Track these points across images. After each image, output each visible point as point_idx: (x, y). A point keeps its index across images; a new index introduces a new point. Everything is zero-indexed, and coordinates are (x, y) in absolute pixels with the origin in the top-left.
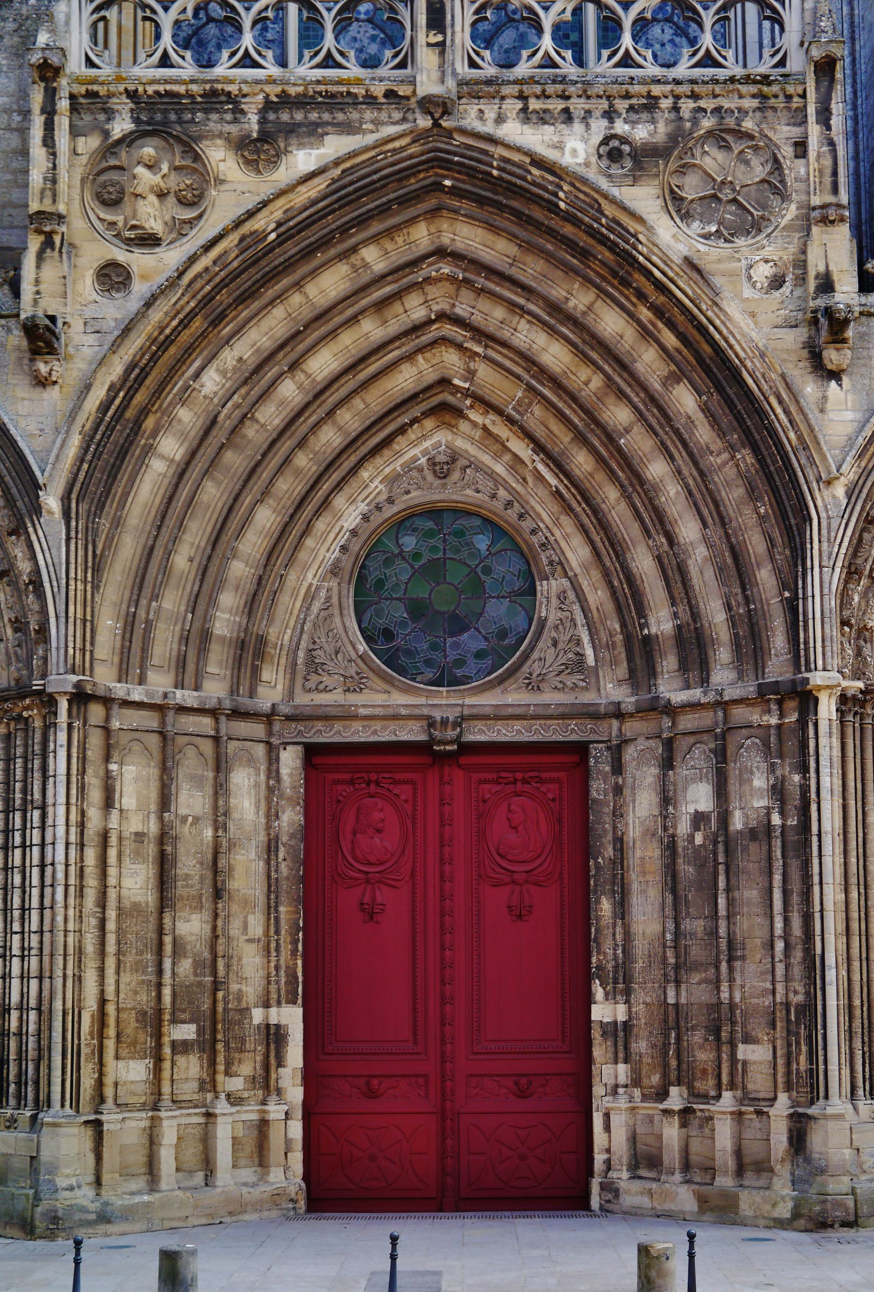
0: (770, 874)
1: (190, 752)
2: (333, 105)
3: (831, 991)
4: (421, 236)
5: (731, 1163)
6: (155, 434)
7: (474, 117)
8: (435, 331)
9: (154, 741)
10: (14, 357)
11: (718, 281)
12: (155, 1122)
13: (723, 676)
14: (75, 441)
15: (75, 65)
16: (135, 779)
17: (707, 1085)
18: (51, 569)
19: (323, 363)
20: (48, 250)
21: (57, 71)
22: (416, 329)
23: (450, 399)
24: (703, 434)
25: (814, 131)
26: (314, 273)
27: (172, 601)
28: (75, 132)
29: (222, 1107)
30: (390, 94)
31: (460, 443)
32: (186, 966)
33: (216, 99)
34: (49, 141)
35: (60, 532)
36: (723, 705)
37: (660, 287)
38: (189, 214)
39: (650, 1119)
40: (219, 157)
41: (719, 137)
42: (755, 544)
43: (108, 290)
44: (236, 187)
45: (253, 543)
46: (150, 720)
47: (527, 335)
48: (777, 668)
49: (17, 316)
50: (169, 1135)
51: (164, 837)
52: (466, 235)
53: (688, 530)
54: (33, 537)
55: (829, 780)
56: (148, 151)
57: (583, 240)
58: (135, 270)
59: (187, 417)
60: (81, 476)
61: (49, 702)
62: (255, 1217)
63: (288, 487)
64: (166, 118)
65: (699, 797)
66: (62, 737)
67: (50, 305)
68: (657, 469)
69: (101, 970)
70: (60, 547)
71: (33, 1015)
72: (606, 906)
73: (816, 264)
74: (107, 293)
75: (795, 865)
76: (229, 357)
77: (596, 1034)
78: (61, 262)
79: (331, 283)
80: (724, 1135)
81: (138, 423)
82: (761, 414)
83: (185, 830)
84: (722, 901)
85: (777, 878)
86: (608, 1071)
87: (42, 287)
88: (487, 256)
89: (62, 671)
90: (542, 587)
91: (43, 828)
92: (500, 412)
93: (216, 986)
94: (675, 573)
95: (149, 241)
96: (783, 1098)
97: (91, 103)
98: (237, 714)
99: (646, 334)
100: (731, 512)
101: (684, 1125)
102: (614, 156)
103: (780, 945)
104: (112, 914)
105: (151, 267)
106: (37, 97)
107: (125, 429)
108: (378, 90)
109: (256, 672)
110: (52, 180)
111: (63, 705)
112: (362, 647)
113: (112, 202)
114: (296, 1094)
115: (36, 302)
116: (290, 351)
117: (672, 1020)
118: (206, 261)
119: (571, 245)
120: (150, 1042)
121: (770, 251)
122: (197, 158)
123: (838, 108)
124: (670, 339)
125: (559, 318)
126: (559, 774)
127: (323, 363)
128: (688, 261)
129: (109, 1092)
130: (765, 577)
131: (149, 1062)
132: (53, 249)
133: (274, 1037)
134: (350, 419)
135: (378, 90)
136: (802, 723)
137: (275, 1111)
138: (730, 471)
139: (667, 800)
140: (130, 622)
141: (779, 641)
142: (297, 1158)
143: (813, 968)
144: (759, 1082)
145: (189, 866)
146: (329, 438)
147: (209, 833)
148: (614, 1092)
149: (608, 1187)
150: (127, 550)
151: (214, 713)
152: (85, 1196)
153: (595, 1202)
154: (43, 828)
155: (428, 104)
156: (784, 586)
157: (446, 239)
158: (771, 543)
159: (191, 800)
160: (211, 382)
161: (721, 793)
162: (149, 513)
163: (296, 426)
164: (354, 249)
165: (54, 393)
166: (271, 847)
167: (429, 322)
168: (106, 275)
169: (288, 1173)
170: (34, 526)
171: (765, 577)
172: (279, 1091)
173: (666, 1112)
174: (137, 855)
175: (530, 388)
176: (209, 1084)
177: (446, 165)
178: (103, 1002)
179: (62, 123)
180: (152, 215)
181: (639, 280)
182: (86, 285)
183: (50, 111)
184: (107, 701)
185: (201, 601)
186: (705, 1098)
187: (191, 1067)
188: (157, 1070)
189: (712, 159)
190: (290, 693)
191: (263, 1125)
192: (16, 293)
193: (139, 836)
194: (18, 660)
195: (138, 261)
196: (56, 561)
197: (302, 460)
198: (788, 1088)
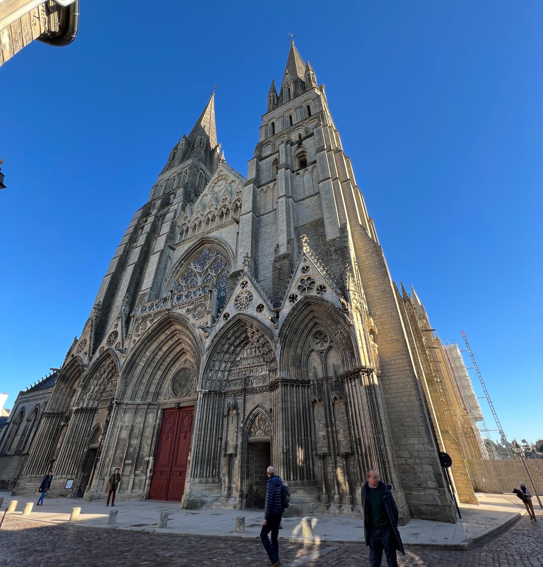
1: (141, 412)
14: (125, 365)
19: (165, 348)
27: (142, 387)
28: (135, 323)
45: (158, 377)
59: (144, 359)
62: (133, 500)
63: (163, 368)
64: (144, 319)
67: (127, 347)
79: (163, 337)
81: (134, 362)
95: (139, 336)
105: (137, 339)
127: (165, 348)
134: (172, 356)
145: (136, 431)
146: (169, 359)
160: (148, 354)
163: (163, 359)
164: (164, 331)
167: (177, 340)
169: (144, 491)
172: (146, 474)
174: (125, 430)
176: (131, 472)
193: (127, 426)
197: (165, 363)
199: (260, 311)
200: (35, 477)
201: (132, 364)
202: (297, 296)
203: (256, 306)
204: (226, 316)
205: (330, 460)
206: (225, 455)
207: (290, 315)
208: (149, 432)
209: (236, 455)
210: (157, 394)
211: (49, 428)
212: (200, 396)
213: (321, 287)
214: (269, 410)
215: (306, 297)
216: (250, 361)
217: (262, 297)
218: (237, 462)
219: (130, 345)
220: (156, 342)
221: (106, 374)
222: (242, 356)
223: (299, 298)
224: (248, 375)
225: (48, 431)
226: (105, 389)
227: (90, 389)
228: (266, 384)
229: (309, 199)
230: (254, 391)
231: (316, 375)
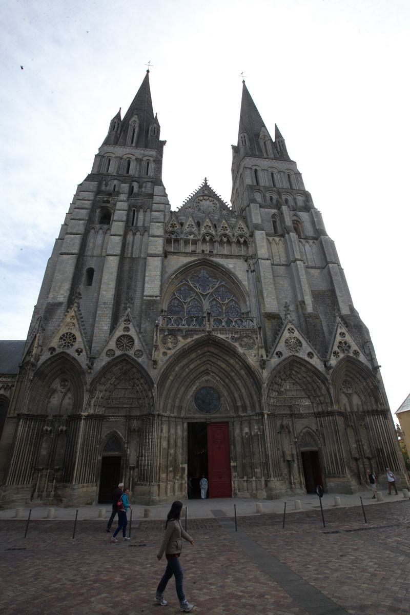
0: (258, 442)
2: (195, 331)
3: (270, 460)
4: (206, 349)
5: (255, 489)
6: (169, 376)
7: (214, 334)
8: (207, 362)
9: (167, 422)
11: (247, 356)
12: (167, 484)
13: (249, 412)
14: (159, 377)
15: (160, 325)
16: (165, 427)
17: (251, 476)
19: (192, 366)
21: (158, 326)
22: (205, 362)
23: (208, 371)
24: (245, 377)
25: (259, 336)
26: (191, 354)
28: (160, 334)
29: (176, 481)
30: (203, 330)
31: (209, 378)
32: (171, 458)
33: (180, 330)
34: (156, 335)
36: (250, 416)
37: (239, 356)
38: (175, 345)
39: (241, 482)
40: (180, 338)
41: (246, 337)
42: (253, 392)
44: (182, 342)
45: (181, 392)
46: (167, 419)
47: (220, 363)
48: (258, 411)
50: (169, 487)
51: (169, 437)
52: (212, 349)
53: (243, 391)
55: (267, 427)
56: (170, 337)
57: (228, 349)
61: (154, 416)
63: (186, 384)
64: (173, 333)
65: (246, 430)
66: (156, 421)
68: (238, 382)
69: (160, 459)
71: (149, 467)
72: (232, 447)
73: (260, 354)
75: (262, 440)
76: (179, 365)
77: (232, 468)
79: (193, 355)
80: (254, 484)
82: (254, 374)
83: (171, 436)
84: (251, 446)
85: (260, 442)
86: (234, 474)
88: (215, 352)
90: (221, 399)
91: (152, 436)
92: (215, 374)
93: (175, 461)
94: (241, 397)
95: (170, 349)
96: (263, 478)
97: (162, 330)
98: (179, 418)
99: (237, 363)
100: (249, 387)
101: (247, 483)
102: (233, 339)
103: (261, 453)
104: (162, 450)
105: (170, 353)
106: (155, 329)
108: (201, 329)
109: (181, 412)
110: (157, 340)
111: (156, 417)
112: (196, 407)
113: (165, 344)
114: (186, 479)
116: (187, 365)
117: (244, 466)
118: (178, 352)
119: (227, 351)
120: (166, 471)
121: (254, 352)
122: (177, 338)
123: (261, 333)
124: (241, 364)
125: (224, 361)
126: (224, 426)
127: (192, 366)
128: (243, 353)
129: (161, 479)
130: (255, 397)
131: (166, 474)
133: (183, 469)
134: (195, 374)
135: (201, 329)
136: (262, 418)
137: (184, 482)
138: (249, 382)
139: (241, 430)
140: (165, 403)
141: (257, 406)
142: (186, 490)
143: (267, 456)
144: (259, 475)
145: (172, 442)
146: (192, 377)
147: (174, 437)
148: (235, 478)
149: (236, 494)
150: (165, 393)
151: (175, 418)
152: (157, 498)
153: (233, 496)
154: (152, 436)
155: (208, 332)
156: (258, 398)
157: (209, 349)
158: (256, 392)
159: (172, 431)
160: (177, 369)
161: (250, 429)
165: (156, 370)
166: (183, 439)
169: (185, 493)
171: (255, 397)
173: (244, 481)
175: (220, 370)
176: (174, 478)
177: (210, 340)
178: (160, 464)
179: (158, 333)
180: (170, 345)
181: (236, 355)
182: (161, 355)
183: (157, 331)
184: (162, 416)
185: (174, 401)
186: (250, 478)
187: (171, 475)
188: (167, 475)
189: (245, 340)
190: (185, 415)
191: (182, 484)
192: (151, 356)
193: (165, 437)
195: (169, 352)
197: (188, 380)
198: (264, 476)
199: (311, 358)
200: (23, 488)
201: (164, 377)
202: (338, 353)
203: (307, 352)
204: (279, 354)
205: (360, 462)
206: (284, 461)
207: (337, 366)
208: (179, 441)
209: (294, 461)
210: (180, 408)
211: (28, 431)
212: (266, 416)
213: (355, 351)
214: (315, 430)
215: (348, 356)
216: (293, 393)
217: (310, 346)
218: (295, 465)
219: (162, 357)
220: (186, 359)
221: (112, 381)
222: (285, 388)
223: (342, 356)
224: (293, 403)
225: (28, 435)
226: (110, 396)
227: (95, 394)
228: (311, 412)
229: (313, 270)
230: (301, 416)
231: (345, 409)
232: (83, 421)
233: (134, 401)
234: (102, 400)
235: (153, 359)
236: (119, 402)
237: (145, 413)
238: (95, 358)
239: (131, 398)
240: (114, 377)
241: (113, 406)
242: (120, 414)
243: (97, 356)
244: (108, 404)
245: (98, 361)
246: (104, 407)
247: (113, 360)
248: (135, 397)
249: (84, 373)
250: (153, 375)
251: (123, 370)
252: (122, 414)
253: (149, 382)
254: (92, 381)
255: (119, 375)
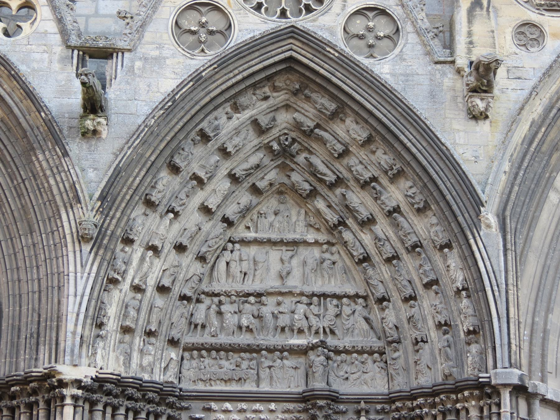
10: (449, 96)
18: (492, 275)
20: (478, 9)
35: (498, 244)
43: (524, 45)
49: (453, 62)
54: (475, 248)
58: (547, 29)
60: (513, 197)
70: (498, 256)
74: (523, 48)
78: (489, 19)
87: (475, 38)
89: (507, 365)
107: (542, 161)
111: (506, 397)
115: (469, 51)
132: (482, 8)
162: (546, 237)
165: (484, 127)
168: (523, 33)
170: (474, 238)
194: (448, 358)
196: (496, 268)
227: (127, 263)
232: (68, 411)
233: (347, 310)
234: (160, 301)
235: (462, 61)
236: (259, 317)
237: (426, 380)
238: (106, 54)
239: (324, 296)
240: (223, 171)
241: (223, 339)
242: (265, 387)
243: (121, 44)
244: (193, 326)
245: (131, 70)
246: (173, 343)
247: (223, 63)
248: (351, 291)
249: (53, 133)
250: (468, 155)
251: (275, 132)
252: (280, 388)
253: (447, 194)
254: (111, 183)
255: (254, 160)
